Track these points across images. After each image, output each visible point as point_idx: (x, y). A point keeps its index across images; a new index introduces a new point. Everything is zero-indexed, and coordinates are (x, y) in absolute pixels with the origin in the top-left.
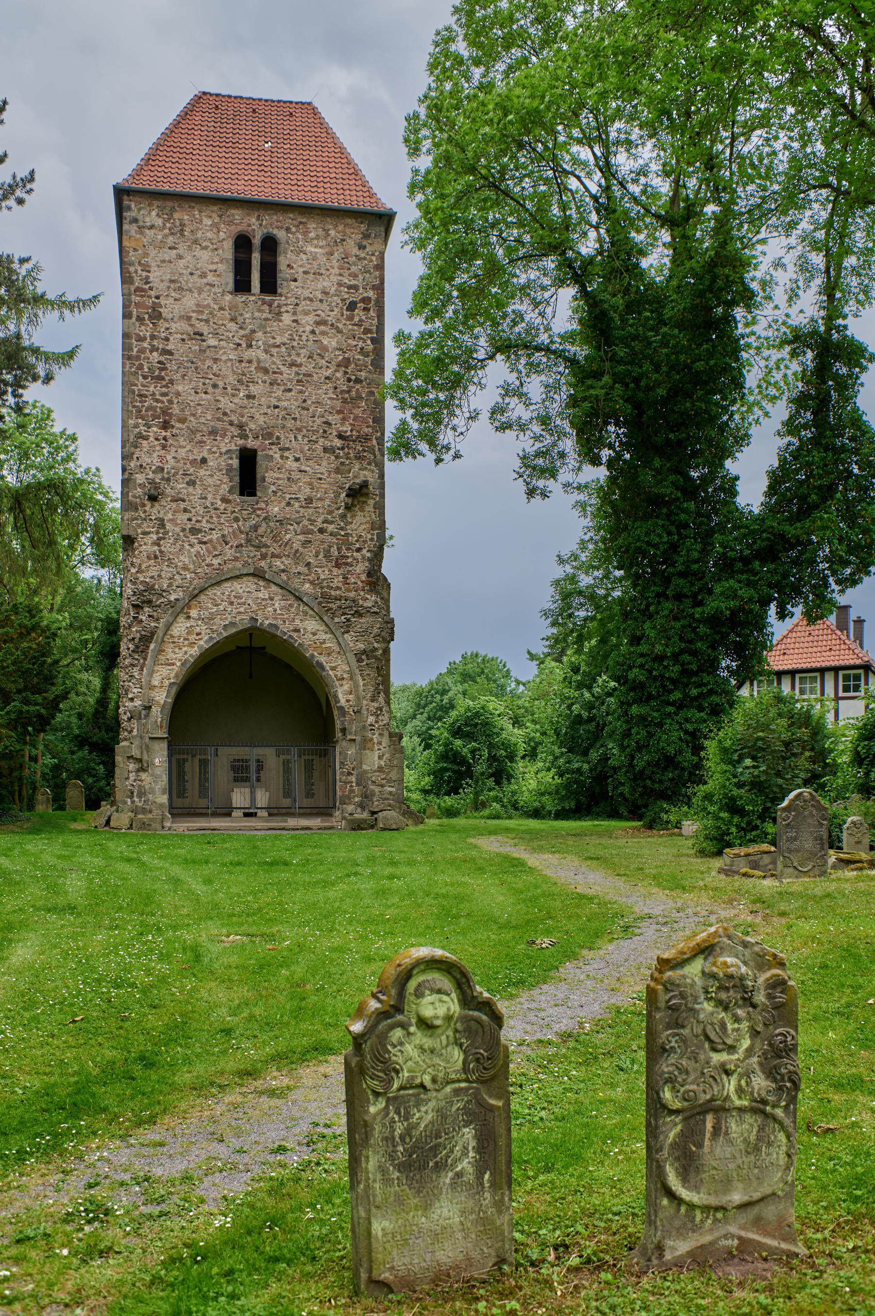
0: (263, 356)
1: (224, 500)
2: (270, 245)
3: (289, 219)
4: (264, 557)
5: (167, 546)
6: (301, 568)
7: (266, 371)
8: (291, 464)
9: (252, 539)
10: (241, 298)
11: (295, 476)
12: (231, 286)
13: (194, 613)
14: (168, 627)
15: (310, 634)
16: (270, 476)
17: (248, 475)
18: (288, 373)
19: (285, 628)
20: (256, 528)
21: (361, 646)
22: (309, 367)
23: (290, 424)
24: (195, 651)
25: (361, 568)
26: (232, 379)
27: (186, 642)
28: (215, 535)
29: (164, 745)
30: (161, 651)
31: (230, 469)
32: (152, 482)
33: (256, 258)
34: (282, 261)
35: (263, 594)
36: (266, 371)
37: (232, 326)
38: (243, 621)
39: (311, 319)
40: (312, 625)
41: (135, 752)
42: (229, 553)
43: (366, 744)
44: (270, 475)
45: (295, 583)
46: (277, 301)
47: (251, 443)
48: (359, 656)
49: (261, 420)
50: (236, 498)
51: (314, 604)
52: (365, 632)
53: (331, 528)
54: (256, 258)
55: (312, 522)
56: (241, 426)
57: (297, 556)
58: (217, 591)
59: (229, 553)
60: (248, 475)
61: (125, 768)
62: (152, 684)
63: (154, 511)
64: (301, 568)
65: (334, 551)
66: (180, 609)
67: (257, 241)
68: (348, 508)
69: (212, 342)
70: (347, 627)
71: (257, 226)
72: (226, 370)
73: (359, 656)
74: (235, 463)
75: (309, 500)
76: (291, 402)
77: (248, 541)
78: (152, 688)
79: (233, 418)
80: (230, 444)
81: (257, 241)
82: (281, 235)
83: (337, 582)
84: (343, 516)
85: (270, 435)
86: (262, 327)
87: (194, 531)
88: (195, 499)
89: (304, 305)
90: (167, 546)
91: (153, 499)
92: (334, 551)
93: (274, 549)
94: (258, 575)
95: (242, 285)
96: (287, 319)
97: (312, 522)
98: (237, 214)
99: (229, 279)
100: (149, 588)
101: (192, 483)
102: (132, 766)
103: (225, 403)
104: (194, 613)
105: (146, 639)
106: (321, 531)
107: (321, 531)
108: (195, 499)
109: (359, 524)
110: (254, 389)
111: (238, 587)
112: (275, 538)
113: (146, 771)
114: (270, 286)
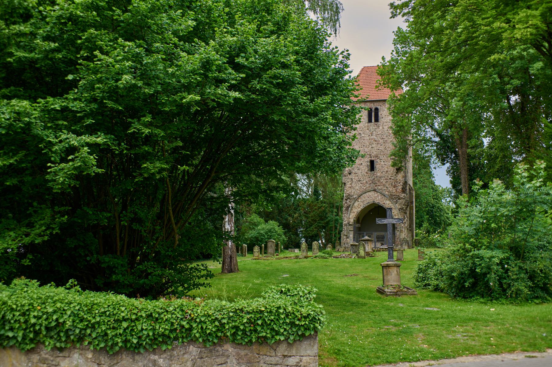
0: (375, 137)
1: (367, 173)
2: (377, 109)
3: (381, 104)
4: (376, 186)
5: (353, 185)
6: (385, 188)
7: (376, 141)
8: (382, 163)
9: (373, 182)
10: (370, 124)
11: (383, 166)
12: (367, 121)
13: (359, 200)
14: (353, 204)
15: (387, 204)
16: (377, 166)
17: (372, 166)
18: (381, 141)
19: (381, 203)
20: (374, 179)
21: (400, 207)
22: (386, 139)
23: (382, 153)
24: (360, 209)
25: (400, 188)
26: (368, 144)
27: (358, 207)
28: (364, 181)
29: (353, 232)
30: (351, 210)
31: (368, 165)
32: (350, 170)
33: (373, 114)
34: (380, 114)
35: (376, 195)
36: (376, 141)
37: (368, 131)
38: (371, 202)
39: (387, 127)
40: (388, 202)
41: (346, 234)
42: (368, 185)
43: (401, 231)
44: (377, 166)
45: (384, 192)
46: (378, 123)
47: (373, 159)
48: (399, 209)
49: (375, 153)
50: (369, 172)
51: (388, 197)
52: (400, 204)
53: (392, 178)
54: (373, 114)
55: (388, 177)
56: (370, 155)
57: (384, 185)
58: (365, 195)
59: (368, 185)
60: (372, 166)
61: (343, 238)
62: (349, 217)
63: (350, 177)
64: (385, 188)
65: (393, 184)
66: (356, 200)
67: (373, 110)
68: (397, 173)
69: (363, 135)
70: (396, 202)
71: (373, 106)
72: (366, 142)
73: (399, 209)
74: (369, 164)
75: (387, 171)
76: (382, 148)
77: (372, 182)
78: (349, 218)
79: (368, 153)
80: (367, 159)
81: (373, 110)
82: (379, 107)
83: (394, 191)
84: (395, 175)
85: (377, 156)
86: (375, 130)
87: (359, 181)
88: (360, 173)
89: (385, 124)
90: (353, 185)
91: (350, 174)
92: (393, 184)
93: (379, 184)
94: (375, 190)
95: (370, 121)
96: (381, 128)
97: (388, 177)
98: (368, 104)
99: (367, 120)
100: (349, 195)
101: (359, 169)
102: (345, 237)
103: (366, 150)
104: (359, 200)
105: (348, 207)
106: (390, 179)
107: (390, 179)
108: (360, 173)
109: (400, 176)
110: (373, 146)
111: (370, 193)
112: (379, 181)
113: (348, 238)
114: (377, 120)
